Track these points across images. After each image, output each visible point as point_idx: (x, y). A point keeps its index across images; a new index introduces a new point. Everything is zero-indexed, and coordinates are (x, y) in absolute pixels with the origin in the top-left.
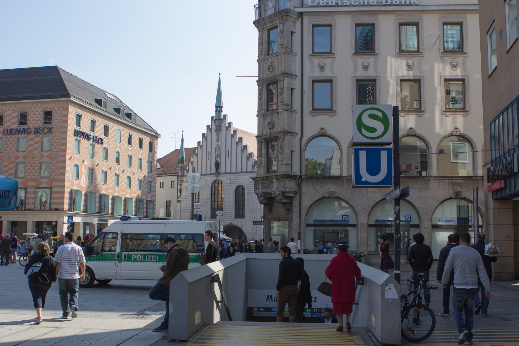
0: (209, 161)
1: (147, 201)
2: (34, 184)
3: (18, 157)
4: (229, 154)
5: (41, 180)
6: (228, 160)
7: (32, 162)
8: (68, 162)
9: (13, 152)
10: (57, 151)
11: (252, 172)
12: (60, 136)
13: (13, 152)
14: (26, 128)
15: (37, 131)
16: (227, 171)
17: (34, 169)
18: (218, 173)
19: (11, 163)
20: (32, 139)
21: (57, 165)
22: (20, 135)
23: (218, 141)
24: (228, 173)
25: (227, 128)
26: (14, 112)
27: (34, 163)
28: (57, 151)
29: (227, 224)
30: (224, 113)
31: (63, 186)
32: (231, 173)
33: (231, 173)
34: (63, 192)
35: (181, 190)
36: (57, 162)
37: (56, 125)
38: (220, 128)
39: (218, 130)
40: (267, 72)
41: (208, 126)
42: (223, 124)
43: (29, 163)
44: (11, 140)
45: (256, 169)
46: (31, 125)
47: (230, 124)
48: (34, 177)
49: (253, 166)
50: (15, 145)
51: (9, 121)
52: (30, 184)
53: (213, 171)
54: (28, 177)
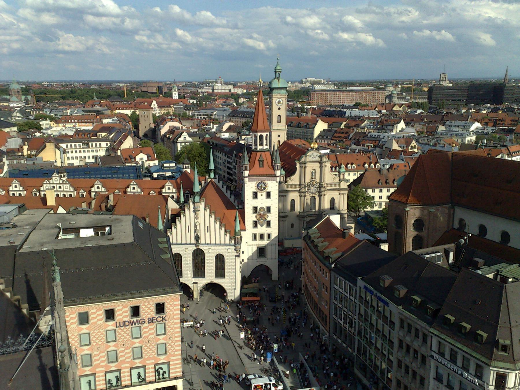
2: (152, 361)
4: (208, 229)
6: (208, 234)
10: (172, 333)
11: (230, 245)
12: (173, 322)
15: (151, 321)
16: (207, 242)
20: (146, 328)
24: (208, 244)
26: (125, 307)
27: (151, 345)
28: (172, 333)
32: (210, 244)
43: (146, 346)
44: (125, 330)
46: (144, 316)
48: (151, 356)
52: (148, 362)
53: (193, 241)
54: (146, 357)
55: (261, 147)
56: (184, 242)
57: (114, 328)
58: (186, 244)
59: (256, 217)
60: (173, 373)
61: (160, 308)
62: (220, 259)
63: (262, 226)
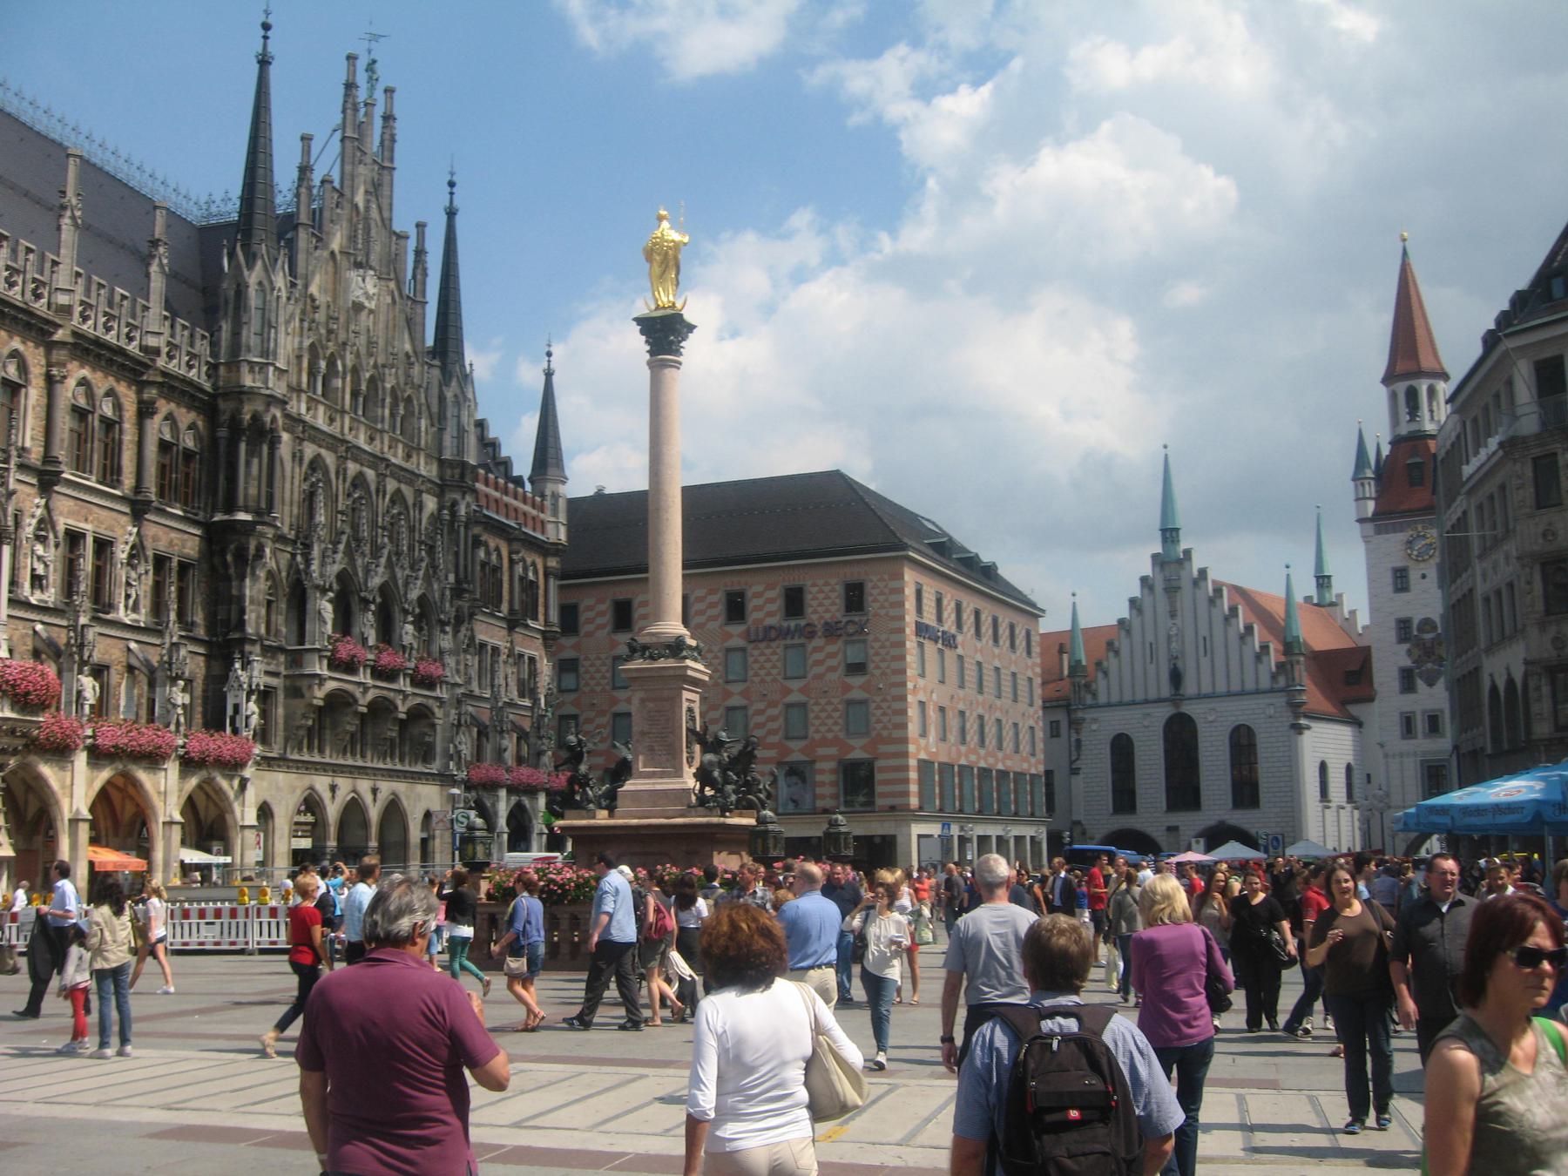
0: (1151, 669)
1: (1032, 776)
2: (833, 751)
3: (788, 692)
4: (1207, 646)
5: (852, 742)
6: (1205, 662)
7: (823, 701)
8: (910, 698)
9: (775, 680)
10: (884, 674)
11: (1271, 691)
13: (775, 680)
14: (803, 623)
15: (832, 631)
17: (829, 717)
18: (1177, 697)
19: (772, 704)
21: (885, 705)
22: (789, 642)
23: (1173, 615)
24: (1206, 697)
25: (1196, 583)
26: (770, 587)
27: (829, 703)
28: (884, 674)
29: (1212, 823)
30: (1183, 546)
31: (905, 755)
32: (1212, 696)
33: (1212, 696)
34: (906, 768)
35: (1078, 741)
36: (884, 700)
37: (876, 615)
38: (1175, 584)
39: (1172, 589)
40: (1540, 541)
41: (1144, 580)
42: (1184, 574)
43: (817, 704)
44: (768, 651)
45: (1282, 681)
47: (1203, 572)
49: (1274, 677)
50: (779, 664)
51: (758, 608)
52: (821, 751)
53: (1166, 691)
54: (817, 736)
55: (1413, 427)
56: (1140, 696)
57: (741, 643)
58: (1146, 702)
59: (1409, 653)
60: (884, 795)
61: (855, 597)
62: (1243, 743)
63: (1431, 684)
